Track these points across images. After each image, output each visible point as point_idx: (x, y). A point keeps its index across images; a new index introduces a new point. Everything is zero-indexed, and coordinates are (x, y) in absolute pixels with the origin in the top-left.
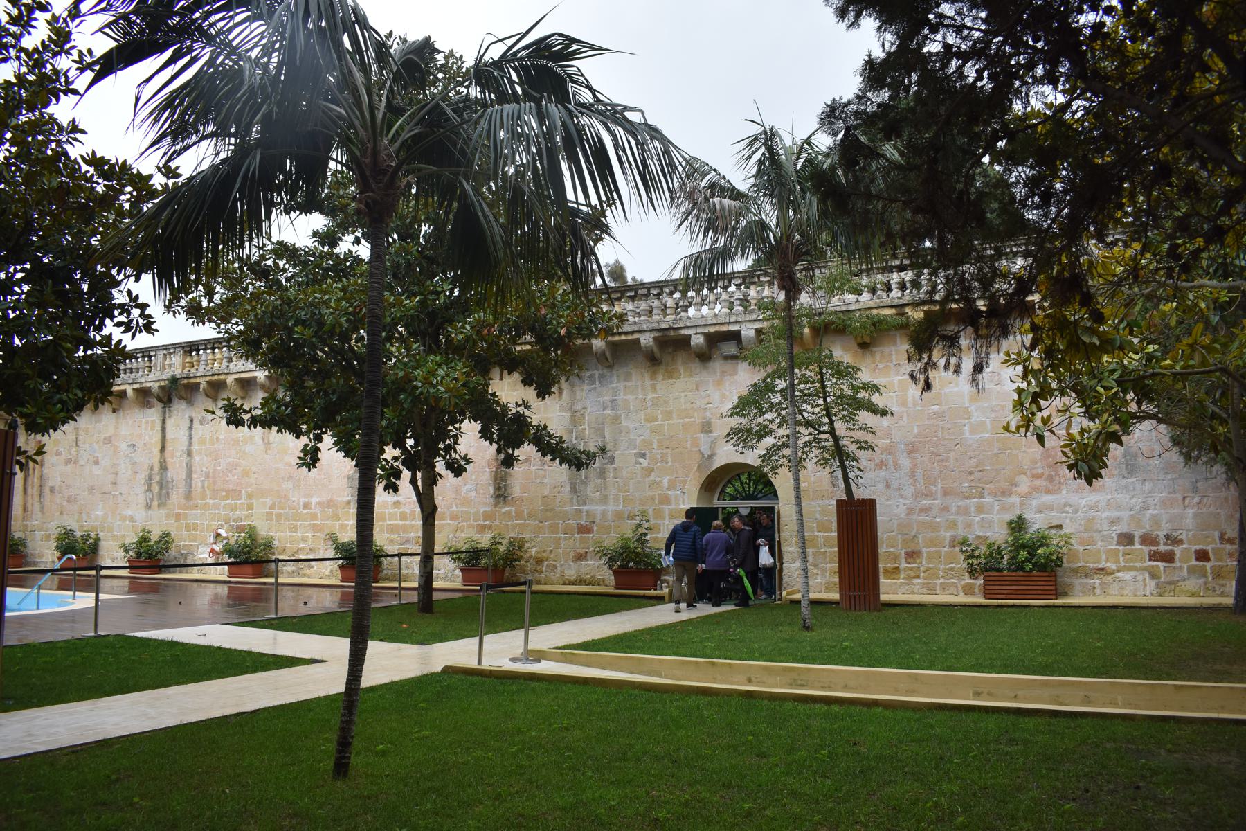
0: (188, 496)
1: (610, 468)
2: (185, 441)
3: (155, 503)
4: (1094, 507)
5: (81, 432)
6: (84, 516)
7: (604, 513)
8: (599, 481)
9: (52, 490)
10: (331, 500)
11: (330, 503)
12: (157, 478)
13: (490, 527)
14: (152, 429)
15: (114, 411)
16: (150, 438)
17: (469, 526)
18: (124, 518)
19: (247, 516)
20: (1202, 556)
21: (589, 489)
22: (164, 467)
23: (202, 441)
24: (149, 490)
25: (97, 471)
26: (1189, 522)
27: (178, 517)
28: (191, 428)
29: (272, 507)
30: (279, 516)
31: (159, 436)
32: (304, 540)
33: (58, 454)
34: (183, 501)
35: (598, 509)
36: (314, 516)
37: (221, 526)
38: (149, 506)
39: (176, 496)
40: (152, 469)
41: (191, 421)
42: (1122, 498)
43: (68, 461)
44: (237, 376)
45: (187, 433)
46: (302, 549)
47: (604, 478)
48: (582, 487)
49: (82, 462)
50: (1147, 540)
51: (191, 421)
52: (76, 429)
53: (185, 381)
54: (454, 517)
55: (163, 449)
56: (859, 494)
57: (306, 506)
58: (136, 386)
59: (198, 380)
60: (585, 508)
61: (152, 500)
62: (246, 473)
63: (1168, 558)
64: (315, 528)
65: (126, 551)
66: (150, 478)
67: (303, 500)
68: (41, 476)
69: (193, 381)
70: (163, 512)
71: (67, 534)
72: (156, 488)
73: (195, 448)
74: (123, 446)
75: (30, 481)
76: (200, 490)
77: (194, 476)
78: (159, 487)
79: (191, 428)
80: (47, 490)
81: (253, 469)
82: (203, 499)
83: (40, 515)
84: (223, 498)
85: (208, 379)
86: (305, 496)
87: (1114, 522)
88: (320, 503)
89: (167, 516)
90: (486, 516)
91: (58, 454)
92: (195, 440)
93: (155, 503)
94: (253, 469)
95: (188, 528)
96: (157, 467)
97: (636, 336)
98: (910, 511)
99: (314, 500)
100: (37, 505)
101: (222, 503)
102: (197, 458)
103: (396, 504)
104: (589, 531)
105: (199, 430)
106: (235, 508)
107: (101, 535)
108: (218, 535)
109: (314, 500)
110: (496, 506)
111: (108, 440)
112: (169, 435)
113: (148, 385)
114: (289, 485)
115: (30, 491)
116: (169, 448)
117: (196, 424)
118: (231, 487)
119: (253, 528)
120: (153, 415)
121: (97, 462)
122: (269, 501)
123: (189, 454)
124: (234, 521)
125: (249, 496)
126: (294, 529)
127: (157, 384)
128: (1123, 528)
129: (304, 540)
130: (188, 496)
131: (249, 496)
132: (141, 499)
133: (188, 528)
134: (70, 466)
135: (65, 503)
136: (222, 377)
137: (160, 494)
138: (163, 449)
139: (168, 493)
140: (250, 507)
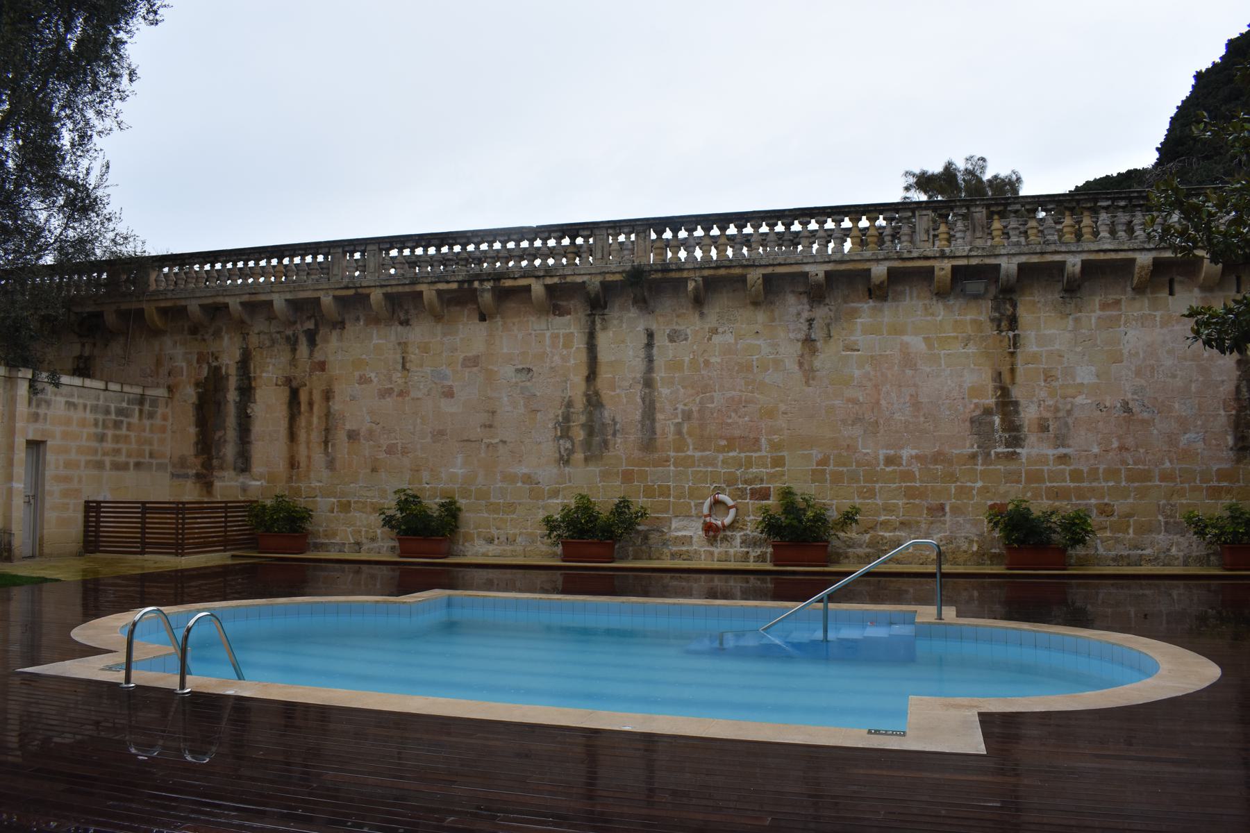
0: (649, 444)
2: (639, 365)
3: (579, 456)
5: (410, 349)
6: (426, 475)
9: (353, 436)
10: (939, 453)
11: (938, 458)
12: (583, 419)
13: (1229, 491)
14: (566, 346)
15: (483, 318)
16: (564, 359)
17: (1193, 489)
18: (512, 479)
19: (772, 477)
22: (594, 402)
23: (675, 365)
24: (565, 434)
25: (447, 406)
27: (627, 477)
28: (649, 345)
29: (824, 462)
30: (837, 478)
31: (583, 356)
32: (887, 509)
33: (364, 380)
34: (637, 454)
36: (907, 476)
37: (719, 490)
38: (565, 460)
39: (623, 448)
40: (570, 404)
41: (650, 335)
43: (385, 393)
44: (769, 270)
45: (642, 354)
46: (885, 524)
49: (413, 394)
51: (650, 335)
52: (403, 345)
53: (659, 275)
54: (1163, 478)
55: (592, 376)
57: (889, 461)
58: (549, 281)
59: (685, 274)
61: (571, 452)
62: (770, 413)
64: (910, 493)
65: (552, 529)
66: (567, 418)
67: (882, 453)
68: (328, 415)
69: (673, 275)
70: (594, 469)
71: (408, 502)
72: (579, 435)
73: (659, 375)
74: (508, 371)
75: (302, 421)
76: (671, 437)
77: (659, 416)
78: (587, 428)
79: (649, 345)
80: (341, 436)
81: (782, 407)
82: (678, 449)
83: (325, 474)
84: (721, 449)
85: (706, 273)
86: (888, 447)
88: (917, 457)
89: (605, 475)
90: (1221, 475)
91: (364, 380)
92: (659, 362)
93: (579, 456)
94: (782, 407)
95: (649, 492)
96: (580, 403)
97: (1130, 255)
99: (906, 453)
100: (318, 457)
101: (721, 457)
102: (664, 391)
103: (1063, 459)
105: (665, 351)
106: (749, 463)
107: (462, 502)
108: (717, 503)
109: (906, 453)
110: (1238, 461)
111: (473, 362)
112: (604, 355)
113: (579, 279)
114: (857, 431)
115: (302, 435)
116: (604, 375)
117: (661, 341)
118: (737, 433)
119: (787, 494)
120: (570, 327)
121: (449, 394)
122: (817, 454)
123: (648, 383)
124: (746, 482)
125: (775, 446)
126: (872, 493)
127: (599, 279)
129: (887, 509)
130: (649, 444)
131: (775, 446)
132: (549, 449)
133: (649, 492)
134: (389, 401)
135: (382, 456)
136: (738, 271)
137: (587, 444)
138: (592, 376)
139: (605, 444)
140: (779, 462)
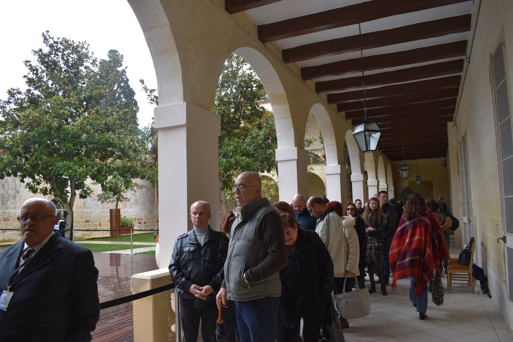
1: (18, 195)
4: (131, 212)
7: (15, 213)
8: (13, 200)
20: (145, 223)
21: (9, 203)
26: (143, 215)
35: (13, 211)
42: (135, 210)
47: (15, 199)
48: (6, 202)
50: (138, 220)
56: (118, 208)
60: (7, 211)
63: (140, 223)
87: (134, 215)
98: (100, 213)
104: (8, 220)
128: (134, 217)
